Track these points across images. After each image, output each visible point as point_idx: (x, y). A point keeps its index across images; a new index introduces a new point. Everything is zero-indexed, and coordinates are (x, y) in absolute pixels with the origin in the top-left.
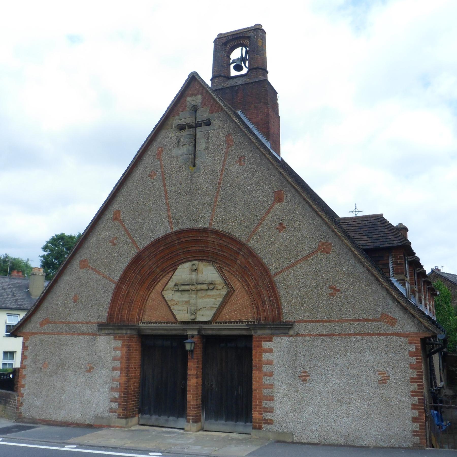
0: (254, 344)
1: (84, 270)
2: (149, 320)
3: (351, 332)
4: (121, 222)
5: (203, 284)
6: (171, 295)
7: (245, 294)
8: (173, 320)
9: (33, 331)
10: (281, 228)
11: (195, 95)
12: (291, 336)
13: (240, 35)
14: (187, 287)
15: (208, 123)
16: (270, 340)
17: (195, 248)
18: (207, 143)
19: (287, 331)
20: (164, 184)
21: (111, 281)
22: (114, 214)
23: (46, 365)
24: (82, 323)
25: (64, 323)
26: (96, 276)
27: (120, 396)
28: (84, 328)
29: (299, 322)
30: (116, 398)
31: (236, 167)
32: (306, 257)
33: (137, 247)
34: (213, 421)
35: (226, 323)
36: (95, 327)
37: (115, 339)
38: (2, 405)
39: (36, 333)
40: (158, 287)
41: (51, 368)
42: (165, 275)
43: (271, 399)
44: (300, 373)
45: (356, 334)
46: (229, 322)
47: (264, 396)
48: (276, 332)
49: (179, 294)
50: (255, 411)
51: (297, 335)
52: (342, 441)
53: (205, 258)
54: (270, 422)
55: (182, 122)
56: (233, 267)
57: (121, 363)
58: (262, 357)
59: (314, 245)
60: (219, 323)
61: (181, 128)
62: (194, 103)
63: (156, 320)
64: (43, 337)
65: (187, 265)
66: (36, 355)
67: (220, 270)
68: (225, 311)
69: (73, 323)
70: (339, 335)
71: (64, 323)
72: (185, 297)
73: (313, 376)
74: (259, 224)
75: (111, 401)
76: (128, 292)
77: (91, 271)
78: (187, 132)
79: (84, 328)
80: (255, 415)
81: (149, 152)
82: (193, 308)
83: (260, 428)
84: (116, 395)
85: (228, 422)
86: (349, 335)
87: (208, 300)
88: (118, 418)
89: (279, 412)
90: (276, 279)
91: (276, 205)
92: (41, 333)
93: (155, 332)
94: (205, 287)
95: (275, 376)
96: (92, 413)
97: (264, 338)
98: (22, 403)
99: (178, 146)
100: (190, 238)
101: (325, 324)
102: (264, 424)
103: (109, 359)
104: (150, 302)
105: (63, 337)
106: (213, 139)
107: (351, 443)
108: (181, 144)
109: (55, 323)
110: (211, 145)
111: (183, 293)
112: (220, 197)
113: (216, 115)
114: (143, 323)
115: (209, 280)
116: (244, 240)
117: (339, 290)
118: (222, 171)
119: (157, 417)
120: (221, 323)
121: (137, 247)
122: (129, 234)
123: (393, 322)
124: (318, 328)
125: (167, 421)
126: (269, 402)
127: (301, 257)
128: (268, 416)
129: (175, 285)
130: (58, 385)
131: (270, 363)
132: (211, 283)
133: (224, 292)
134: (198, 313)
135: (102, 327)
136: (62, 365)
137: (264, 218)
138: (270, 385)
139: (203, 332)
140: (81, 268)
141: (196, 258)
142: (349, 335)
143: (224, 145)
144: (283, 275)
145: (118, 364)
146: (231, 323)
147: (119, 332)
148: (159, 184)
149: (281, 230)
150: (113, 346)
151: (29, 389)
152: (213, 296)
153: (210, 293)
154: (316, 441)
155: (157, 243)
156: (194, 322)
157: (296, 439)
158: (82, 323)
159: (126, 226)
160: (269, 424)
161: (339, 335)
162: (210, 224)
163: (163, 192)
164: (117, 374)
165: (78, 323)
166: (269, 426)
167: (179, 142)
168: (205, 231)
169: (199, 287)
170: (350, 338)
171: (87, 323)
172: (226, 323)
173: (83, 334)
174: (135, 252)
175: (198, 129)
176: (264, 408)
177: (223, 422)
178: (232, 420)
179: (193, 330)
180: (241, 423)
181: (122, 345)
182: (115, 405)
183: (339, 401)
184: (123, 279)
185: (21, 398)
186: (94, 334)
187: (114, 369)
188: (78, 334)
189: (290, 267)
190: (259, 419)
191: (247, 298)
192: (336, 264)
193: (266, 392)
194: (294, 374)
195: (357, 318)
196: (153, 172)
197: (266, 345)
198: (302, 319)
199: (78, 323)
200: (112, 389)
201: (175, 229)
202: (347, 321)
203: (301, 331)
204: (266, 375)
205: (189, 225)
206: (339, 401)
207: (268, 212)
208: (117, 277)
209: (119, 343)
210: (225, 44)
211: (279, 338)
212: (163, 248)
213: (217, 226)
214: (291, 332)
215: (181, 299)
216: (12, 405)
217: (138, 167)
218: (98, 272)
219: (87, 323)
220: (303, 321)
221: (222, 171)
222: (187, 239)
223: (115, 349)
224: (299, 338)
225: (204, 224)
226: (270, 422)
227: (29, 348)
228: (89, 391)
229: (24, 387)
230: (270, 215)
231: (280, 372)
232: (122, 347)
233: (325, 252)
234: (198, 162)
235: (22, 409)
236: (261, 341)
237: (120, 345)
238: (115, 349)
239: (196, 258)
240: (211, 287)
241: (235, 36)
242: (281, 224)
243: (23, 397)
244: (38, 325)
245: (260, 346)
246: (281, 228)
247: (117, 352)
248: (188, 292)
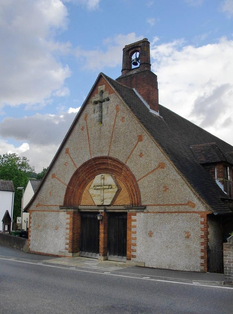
0: (128, 217)
1: (53, 179)
2: (83, 204)
3: (173, 211)
4: (69, 154)
5: (106, 185)
6: (92, 191)
7: (126, 190)
8: (94, 205)
10: (141, 155)
11: (102, 85)
12: (145, 213)
13: (136, 46)
14: (99, 187)
15: (108, 100)
16: (135, 215)
17: (102, 167)
18: (107, 110)
19: (143, 210)
20: (88, 133)
21: (65, 184)
22: (66, 150)
23: (39, 226)
24: (53, 206)
25: (46, 205)
26: (58, 182)
28: (54, 208)
29: (149, 205)
31: (121, 123)
32: (153, 171)
33: (76, 167)
34: (112, 256)
35: (118, 206)
37: (67, 214)
39: (34, 211)
40: (87, 188)
41: (41, 228)
42: (90, 181)
43: (135, 245)
44: (149, 232)
45: (175, 212)
46: (119, 206)
47: (132, 243)
48: (138, 211)
49: (96, 190)
50: (128, 251)
51: (148, 212)
52: (167, 267)
53: (108, 172)
54: (134, 257)
55: (96, 100)
56: (121, 177)
57: (70, 225)
58: (131, 224)
59: (157, 164)
60: (114, 206)
61: (96, 103)
62: (101, 89)
63: (86, 204)
64: (37, 212)
65: (99, 176)
66: (35, 221)
67: (115, 179)
68: (117, 200)
70: (168, 212)
71: (46, 205)
72: (99, 192)
73: (154, 234)
74: (131, 154)
75: (66, 244)
76: (73, 190)
77: (57, 180)
78: (98, 105)
79: (54, 208)
80: (128, 253)
81: (81, 117)
82: (102, 198)
83: (130, 259)
84: (68, 241)
85: (119, 257)
86: (172, 212)
87: (109, 194)
88: (69, 252)
89: (139, 252)
90: (139, 183)
91: (139, 143)
92: (37, 211)
93: (85, 210)
94: (107, 187)
95: (137, 233)
96: (58, 249)
97: (133, 214)
99: (94, 113)
100: (100, 162)
101: (161, 206)
102: (132, 257)
103: (65, 224)
104: (83, 195)
105: (45, 213)
106: (110, 108)
107: (171, 269)
108: (96, 111)
110: (109, 111)
111: (97, 190)
112: (113, 140)
113: (112, 95)
114: (81, 206)
115: (109, 184)
116: (124, 162)
117: (168, 189)
118: (114, 125)
119: (88, 253)
120: (115, 206)
121: (76, 167)
123: (194, 206)
124: (157, 209)
125: (92, 255)
126: (134, 247)
127: (151, 171)
128: (133, 253)
129: (94, 186)
130: (44, 236)
131: (135, 227)
132: (109, 185)
133: (116, 190)
134: (104, 200)
135: (61, 207)
136: (45, 226)
137: (133, 150)
138: (135, 238)
139: (107, 210)
140: (52, 178)
141: (104, 172)
142: (172, 212)
143: (115, 111)
144: (142, 180)
145: (68, 226)
146: (120, 206)
148: (86, 133)
149: (141, 157)
150: (66, 217)
153: (110, 190)
154: (155, 267)
155: (85, 164)
156: (102, 205)
157: (146, 266)
158: (53, 206)
159: (71, 156)
160: (134, 257)
161: (168, 212)
162: (108, 154)
163: (87, 138)
164: (68, 231)
165: (52, 206)
166: (134, 259)
167: (95, 110)
168: (106, 158)
169: (105, 187)
170: (173, 214)
171: (55, 206)
172: (118, 206)
173: (54, 211)
174: (75, 169)
175: (103, 103)
177: (117, 256)
178: (121, 256)
179: (102, 209)
180: (125, 257)
181: (70, 217)
182: (67, 246)
183: (167, 247)
184: (70, 183)
186: (58, 211)
187: (67, 229)
188: (51, 211)
189: (146, 176)
190: (130, 255)
191: (127, 193)
192: (167, 175)
193: (133, 242)
194: (146, 232)
195: (177, 203)
196: (83, 127)
197: (133, 217)
198: (150, 204)
200: (66, 238)
201: (93, 157)
202: (172, 205)
203: (150, 210)
204: (133, 233)
205: (99, 155)
206: (167, 247)
207: (135, 147)
208: (67, 182)
209: (69, 216)
210: (128, 51)
211: (139, 214)
212: (88, 167)
213: (111, 155)
214: (145, 211)
215: (96, 194)
217: (77, 125)
218: (59, 180)
219: (55, 206)
220: (151, 205)
221: (114, 125)
223: (67, 218)
224: (149, 214)
225: (105, 154)
226: (134, 257)
228: (56, 239)
230: (136, 149)
231: (139, 231)
233: (162, 168)
234: (103, 121)
235: (30, 247)
236: (131, 215)
238: (67, 218)
239: (104, 172)
240: (110, 187)
241: (133, 46)
242: (141, 153)
245: (131, 218)
246: (141, 155)
247: (68, 220)
248: (100, 190)
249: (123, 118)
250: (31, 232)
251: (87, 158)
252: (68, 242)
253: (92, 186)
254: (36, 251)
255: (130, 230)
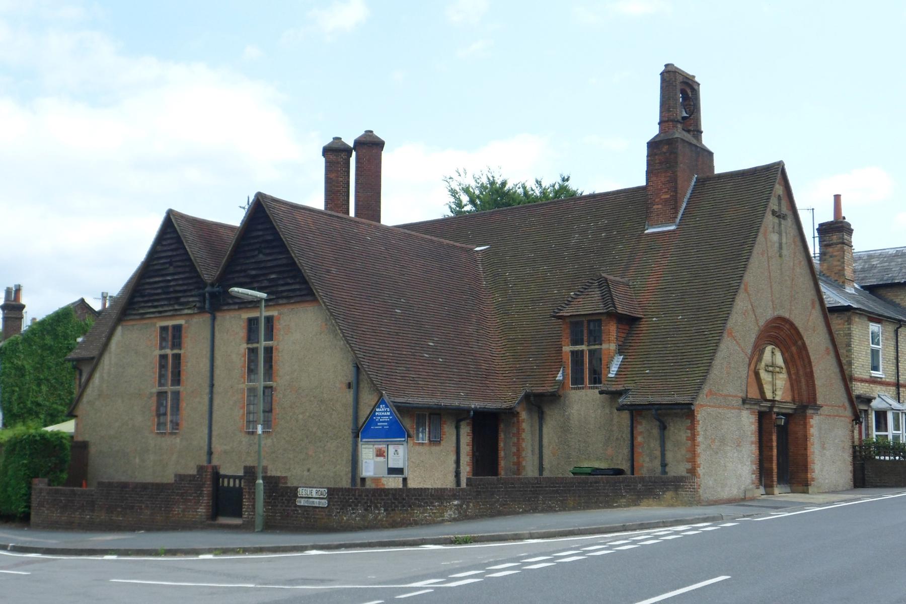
4: (749, 295)
9: (702, 403)
23: (713, 441)
26: (737, 348)
27: (757, 469)
30: (754, 470)
36: (740, 402)
38: (671, 492)
51: (821, 414)
64: (709, 410)
69: (727, 395)
91: (814, 311)
92: (707, 405)
94: (778, 369)
95: (815, 446)
96: (743, 486)
98: (699, 485)
105: (720, 410)
109: (716, 394)
122: (754, 310)
136: (723, 441)
143: (793, 246)
147: (753, 407)
150: (751, 420)
151: (704, 468)
152: (781, 378)
176: (812, 470)
182: (754, 476)
185: (699, 479)
186: (739, 409)
199: (730, 396)
201: (775, 314)
203: (822, 413)
216: (690, 488)
222: (774, 325)
226: (813, 480)
227: (701, 422)
229: (699, 467)
232: (755, 422)
235: (701, 491)
237: (754, 421)
243: (699, 478)
244: (705, 396)
245: (809, 422)
249: (800, 262)
250: (702, 456)
251: (769, 314)
252: (755, 469)
253: (763, 364)
254: (711, 498)
255: (809, 441)
